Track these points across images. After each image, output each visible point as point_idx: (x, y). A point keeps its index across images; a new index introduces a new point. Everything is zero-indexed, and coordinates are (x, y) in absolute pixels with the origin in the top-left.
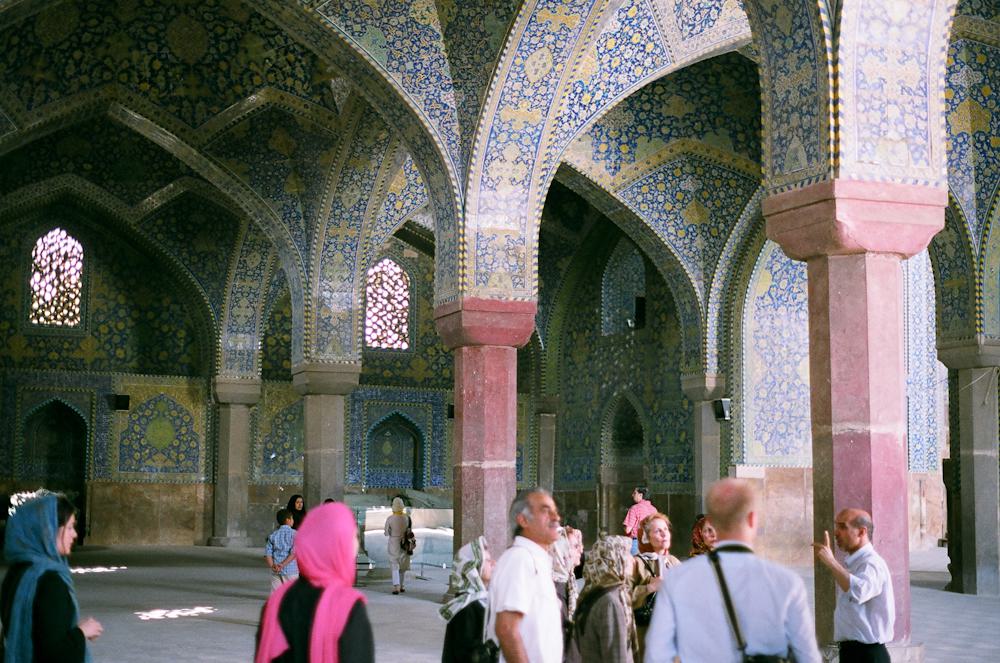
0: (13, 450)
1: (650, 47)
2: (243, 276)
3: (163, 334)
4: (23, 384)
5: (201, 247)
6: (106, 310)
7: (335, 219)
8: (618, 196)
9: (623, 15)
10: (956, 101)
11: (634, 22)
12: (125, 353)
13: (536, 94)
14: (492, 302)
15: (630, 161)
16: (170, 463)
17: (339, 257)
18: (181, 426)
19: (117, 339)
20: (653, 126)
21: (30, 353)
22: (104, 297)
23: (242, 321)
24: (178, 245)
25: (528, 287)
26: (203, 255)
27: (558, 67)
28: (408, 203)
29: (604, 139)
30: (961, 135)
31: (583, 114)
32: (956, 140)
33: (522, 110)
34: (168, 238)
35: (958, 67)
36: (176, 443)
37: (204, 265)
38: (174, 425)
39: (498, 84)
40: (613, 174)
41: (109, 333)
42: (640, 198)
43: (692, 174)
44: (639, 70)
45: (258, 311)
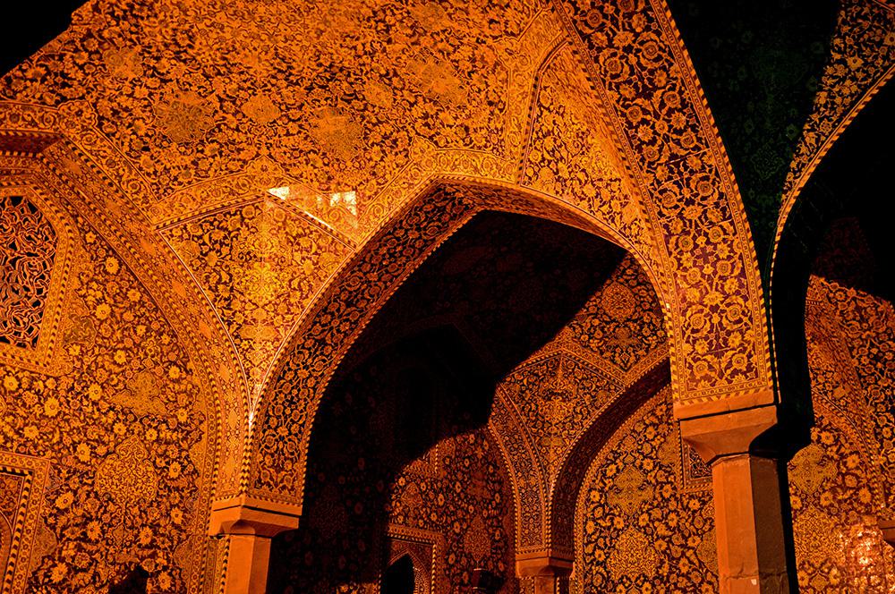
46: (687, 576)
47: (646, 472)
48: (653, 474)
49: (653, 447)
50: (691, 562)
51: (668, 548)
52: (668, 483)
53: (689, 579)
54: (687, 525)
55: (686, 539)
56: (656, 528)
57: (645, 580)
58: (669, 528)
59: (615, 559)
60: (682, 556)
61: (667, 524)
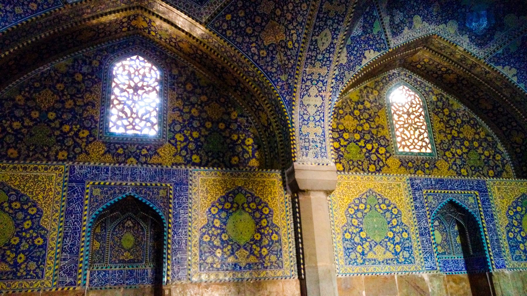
0: (77, 253)
3: (234, 142)
4: (92, 179)
5: (269, 40)
6: (181, 121)
12: (201, 158)
16: (252, 259)
18: (261, 219)
19: (192, 146)
22: (179, 110)
24: (247, 40)
26: (271, 48)
34: (236, 33)
36: (258, 237)
37: (273, 58)
38: (254, 217)
41: (185, 140)
45: (327, 99)
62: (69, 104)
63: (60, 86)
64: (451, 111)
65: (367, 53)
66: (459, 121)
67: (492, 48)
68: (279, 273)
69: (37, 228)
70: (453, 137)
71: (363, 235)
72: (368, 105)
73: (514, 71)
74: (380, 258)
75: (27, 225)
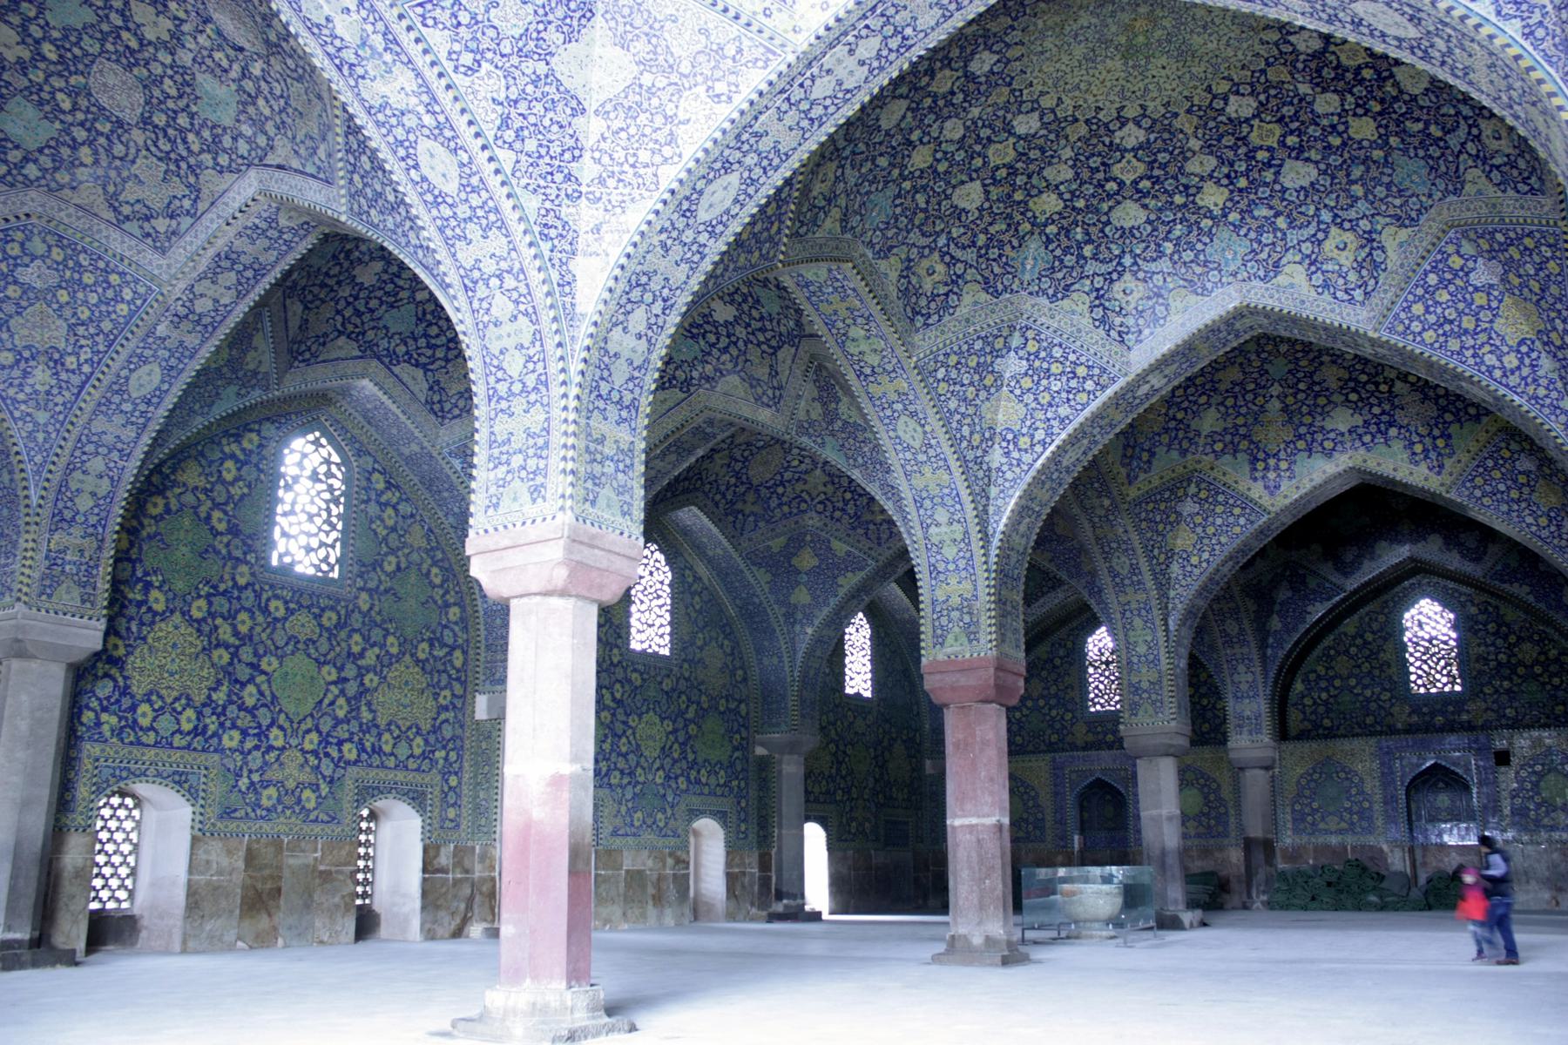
1: (1081, 371)
2: (1229, 643)
7: (1120, 588)
8: (1452, 495)
9: (1021, 353)
10: (1494, 304)
11: (1043, 354)
13: (929, 458)
14: (949, 662)
15: (1450, 456)
17: (1138, 622)
20: (1459, 410)
21: (1090, 738)
23: (1244, 687)
25: (982, 641)
27: (928, 428)
28: (1206, 556)
29: (1415, 438)
30: (1522, 342)
31: (1027, 458)
32: (1518, 351)
33: (929, 475)
35: (1471, 264)
36: (1206, 810)
39: (893, 459)
40: (1439, 473)
42: (1478, 493)
43: (1523, 450)
44: (1082, 397)
46: (251, 711)
47: (216, 533)
48: (225, 540)
49: (230, 497)
50: (261, 693)
51: (231, 664)
52: (247, 563)
53: (254, 716)
54: (264, 636)
55: (260, 657)
56: (216, 628)
57: (188, 705)
58: (236, 633)
59: (143, 660)
60: (249, 681)
61: (234, 627)
62: (1053, 690)
63: (1044, 673)
64: (1499, 626)
65: (1310, 609)
66: (1512, 639)
67: (1489, 564)
68: (1226, 842)
69: (1037, 806)
70: (1500, 664)
71: (1315, 805)
72: (1369, 637)
73: (1526, 589)
74: (1333, 827)
75: (1031, 803)
